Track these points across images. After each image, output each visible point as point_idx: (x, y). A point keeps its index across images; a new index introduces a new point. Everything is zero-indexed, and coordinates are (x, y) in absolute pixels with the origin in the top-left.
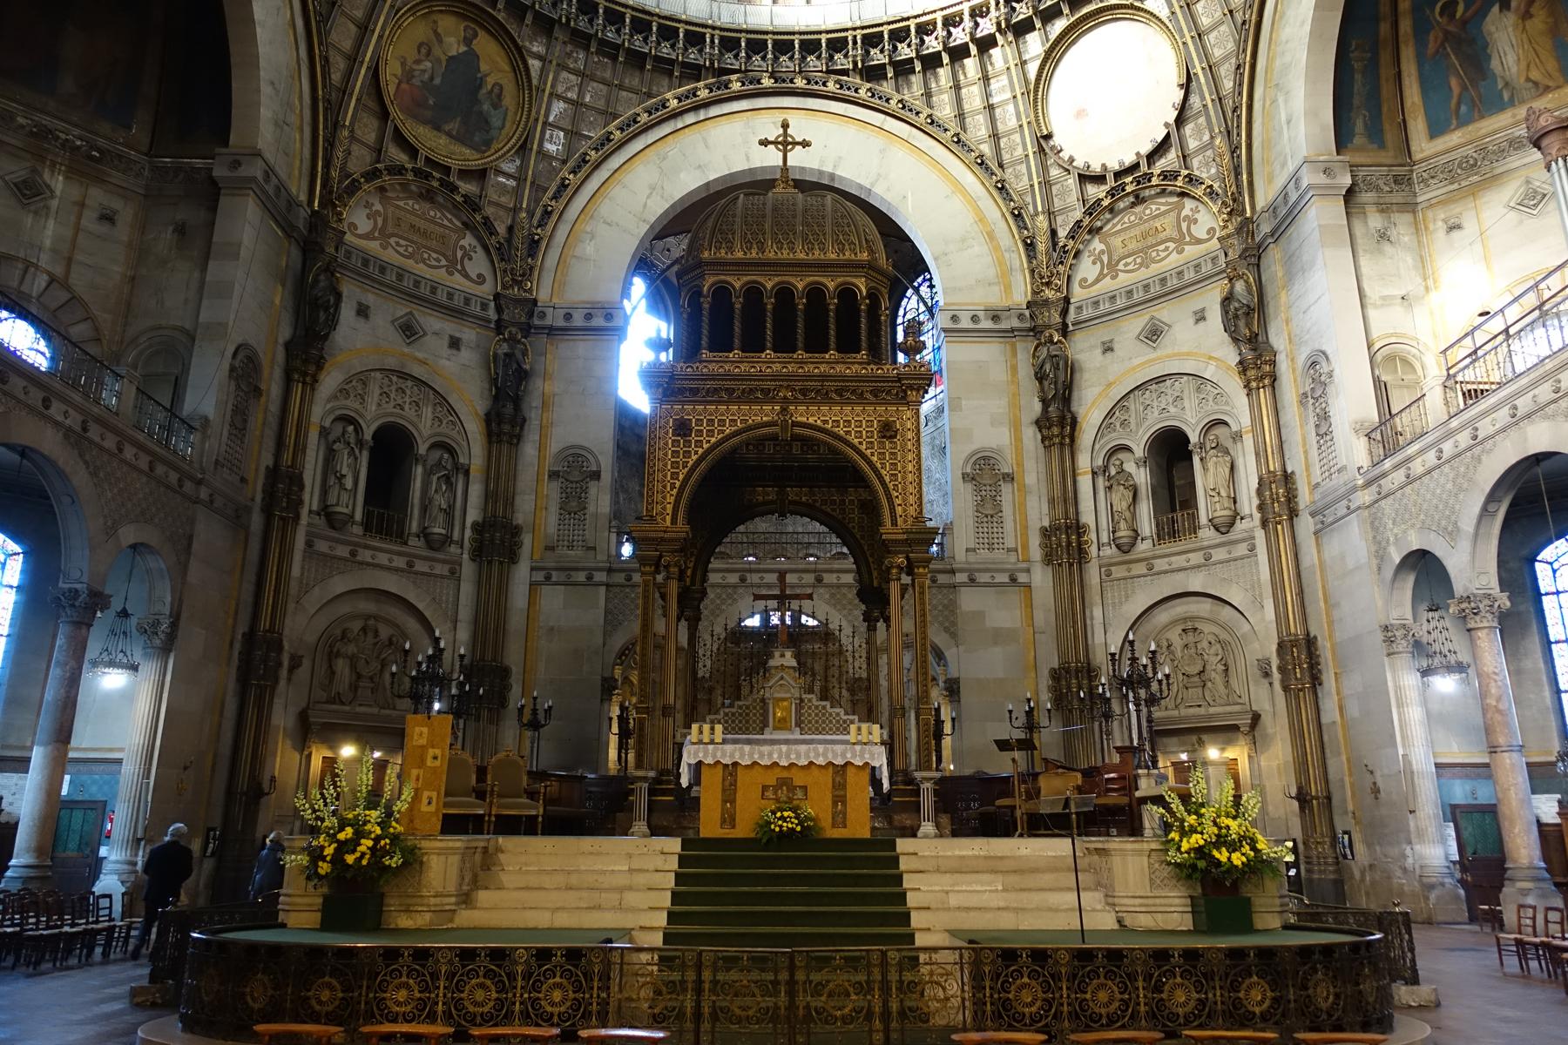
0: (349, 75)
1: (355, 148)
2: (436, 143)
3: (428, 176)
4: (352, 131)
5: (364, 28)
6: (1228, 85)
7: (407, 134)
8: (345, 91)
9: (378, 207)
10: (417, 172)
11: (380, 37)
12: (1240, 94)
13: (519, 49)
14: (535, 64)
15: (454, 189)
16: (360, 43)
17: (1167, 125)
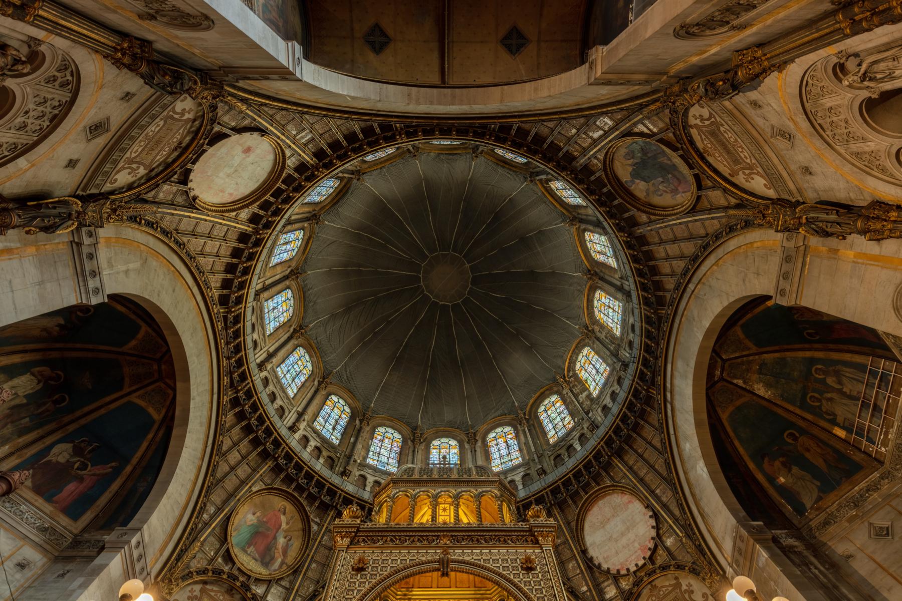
0: (212, 517)
1: (199, 555)
2: (247, 561)
3: (236, 578)
4: (202, 544)
5: (231, 496)
6: (677, 512)
7: (231, 551)
8: (207, 524)
9: (197, 593)
10: (230, 575)
11: (239, 500)
12: (685, 513)
13: (308, 517)
14: (315, 527)
15: (248, 589)
16: (225, 502)
17: (653, 538)
